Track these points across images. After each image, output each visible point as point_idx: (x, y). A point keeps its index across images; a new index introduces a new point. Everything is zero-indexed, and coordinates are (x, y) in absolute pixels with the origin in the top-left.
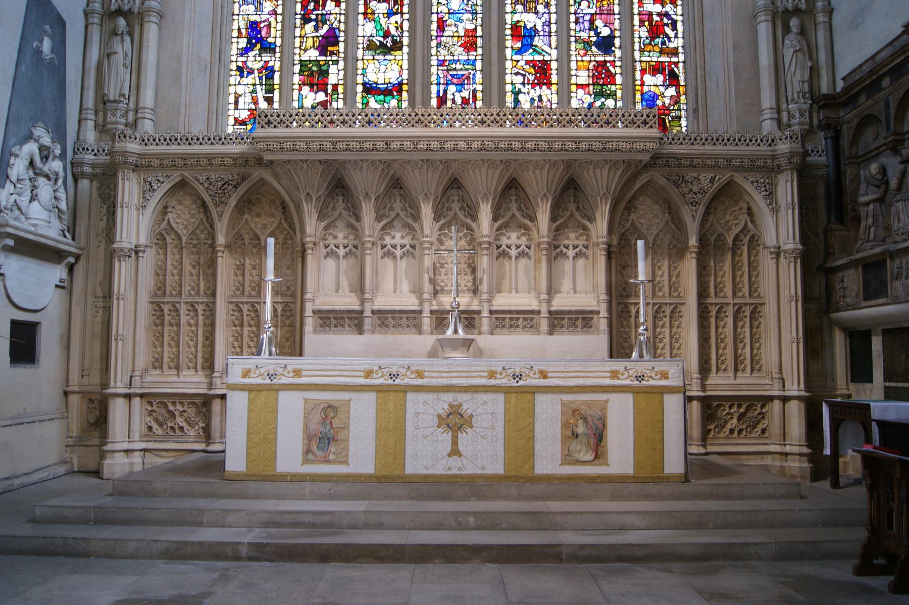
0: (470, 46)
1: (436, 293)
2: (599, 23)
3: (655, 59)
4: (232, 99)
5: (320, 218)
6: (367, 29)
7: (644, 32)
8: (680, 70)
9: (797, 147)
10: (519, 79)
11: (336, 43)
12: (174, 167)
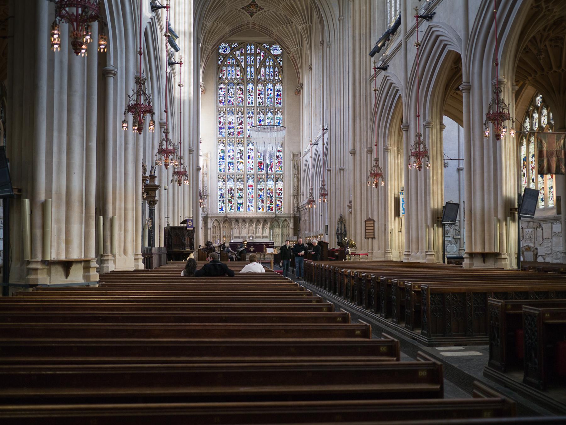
0: (252, 197)
1: (248, 234)
2: (271, 194)
6: (238, 195)
8: (282, 201)
9: (293, 215)
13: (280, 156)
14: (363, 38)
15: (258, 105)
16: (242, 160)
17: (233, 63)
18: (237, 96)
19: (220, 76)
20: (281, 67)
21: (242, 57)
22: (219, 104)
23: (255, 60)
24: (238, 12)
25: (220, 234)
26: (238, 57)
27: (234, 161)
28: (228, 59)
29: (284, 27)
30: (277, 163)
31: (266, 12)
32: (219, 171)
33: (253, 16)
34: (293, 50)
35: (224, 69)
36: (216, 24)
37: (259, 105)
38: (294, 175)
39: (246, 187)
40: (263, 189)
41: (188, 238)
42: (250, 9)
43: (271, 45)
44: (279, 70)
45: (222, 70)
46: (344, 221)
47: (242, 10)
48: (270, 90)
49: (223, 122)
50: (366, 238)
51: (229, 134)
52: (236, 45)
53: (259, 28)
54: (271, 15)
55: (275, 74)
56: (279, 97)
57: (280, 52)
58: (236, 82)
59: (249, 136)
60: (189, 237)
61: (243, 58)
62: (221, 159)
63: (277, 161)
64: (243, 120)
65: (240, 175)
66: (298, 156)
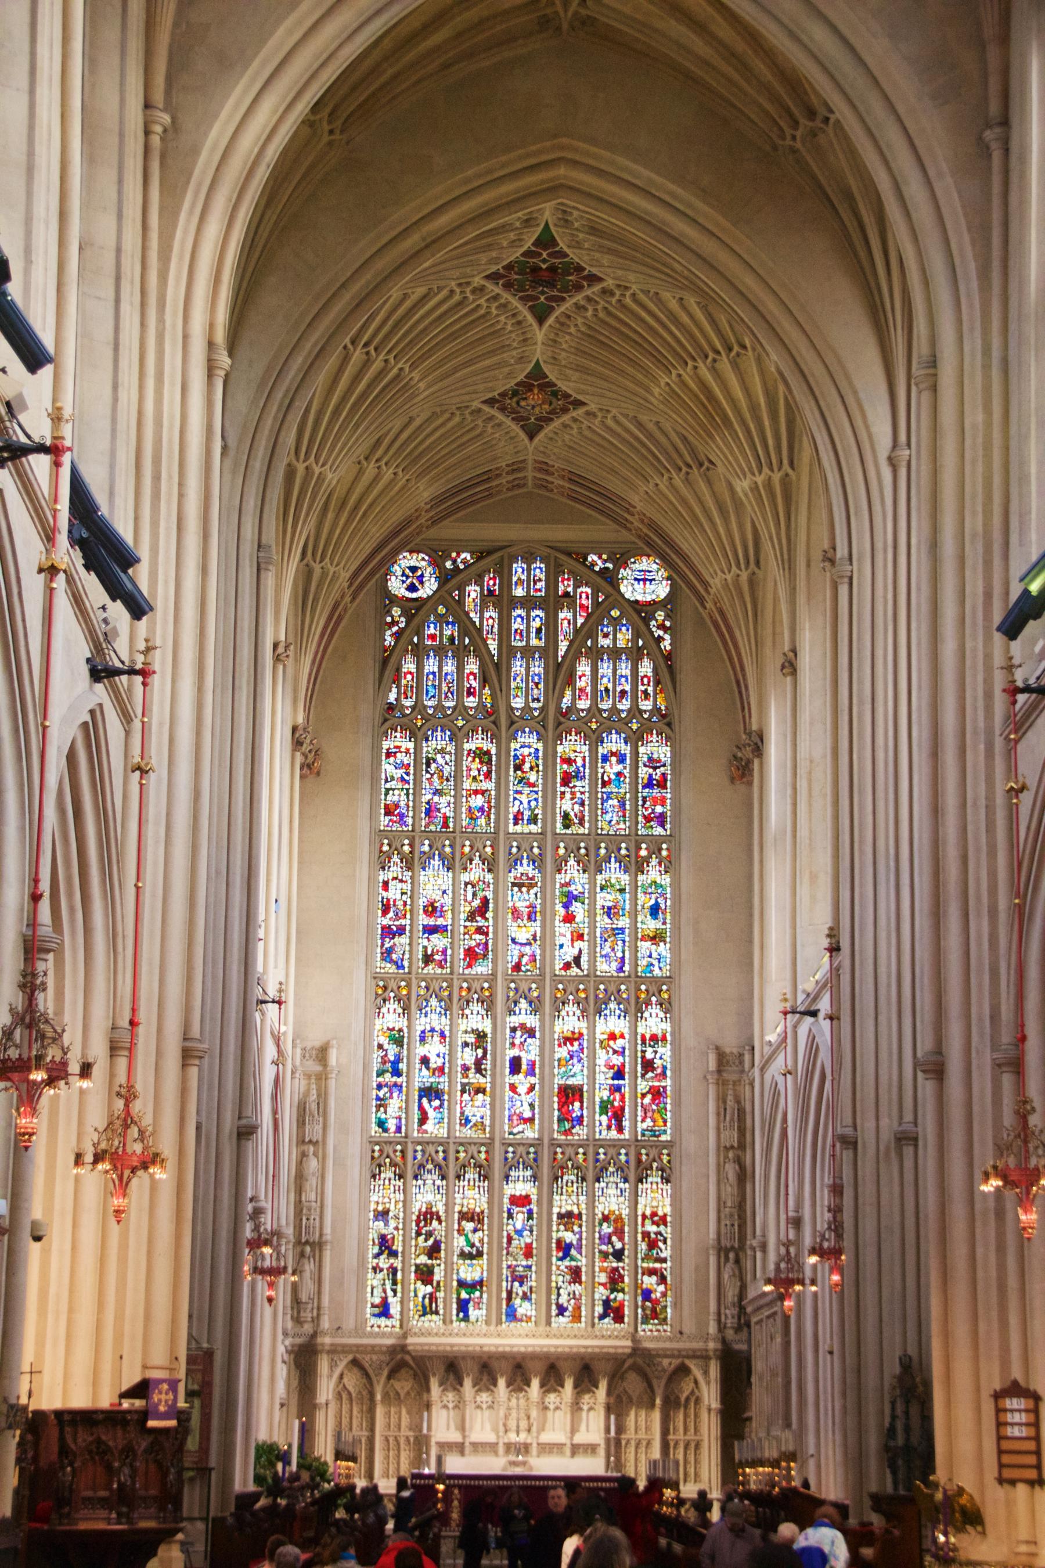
1: (506, 1431)
2: (614, 1239)
3: (651, 1265)
4: (369, 1289)
5: (441, 1385)
6: (459, 1242)
7: (643, 1246)
8: (667, 1274)
10: (561, 1278)
11: (439, 1251)
12: (350, 1352)
13: (658, 1062)
14: (974, 554)
15: (559, 825)
16: (482, 1080)
17: (452, 639)
18: (467, 784)
19: (392, 697)
20: (668, 657)
21: (491, 613)
22: (384, 820)
23: (551, 627)
24: (469, 418)
25: (372, 1429)
26: (472, 615)
27: (443, 1083)
28: (425, 621)
29: (678, 481)
30: (644, 1096)
31: (595, 415)
32: (375, 1127)
33: (541, 436)
34: (717, 581)
35: (409, 665)
36: (371, 470)
37: (566, 826)
38: (723, 1149)
39: (501, 1204)
40: (579, 1216)
41: (152, 1467)
42: (523, 403)
43: (621, 560)
44: (655, 670)
45: (398, 669)
46: (921, 1389)
47: (486, 408)
48: (614, 759)
49: (400, 904)
50: (1001, 1481)
51: (428, 959)
52: (464, 561)
53: (567, 485)
54: (619, 430)
55: (641, 688)
56: (656, 792)
57: (662, 590)
58: (460, 723)
59: (517, 967)
60: (156, 1461)
61: (495, 615)
62: (388, 1075)
63: (643, 1086)
64: (490, 895)
65: (473, 1149)
66: (741, 1062)
